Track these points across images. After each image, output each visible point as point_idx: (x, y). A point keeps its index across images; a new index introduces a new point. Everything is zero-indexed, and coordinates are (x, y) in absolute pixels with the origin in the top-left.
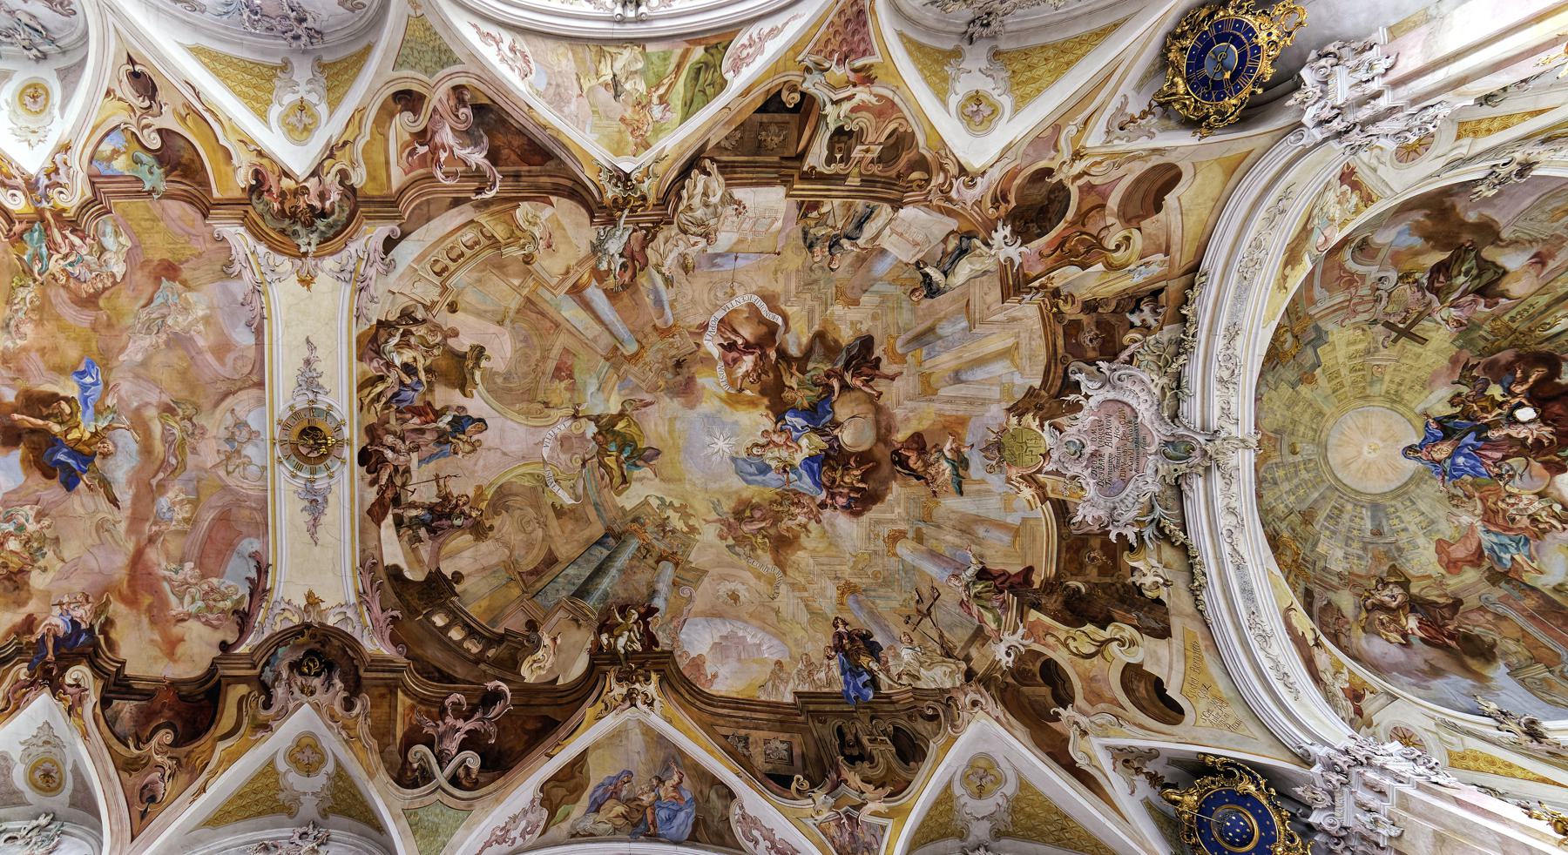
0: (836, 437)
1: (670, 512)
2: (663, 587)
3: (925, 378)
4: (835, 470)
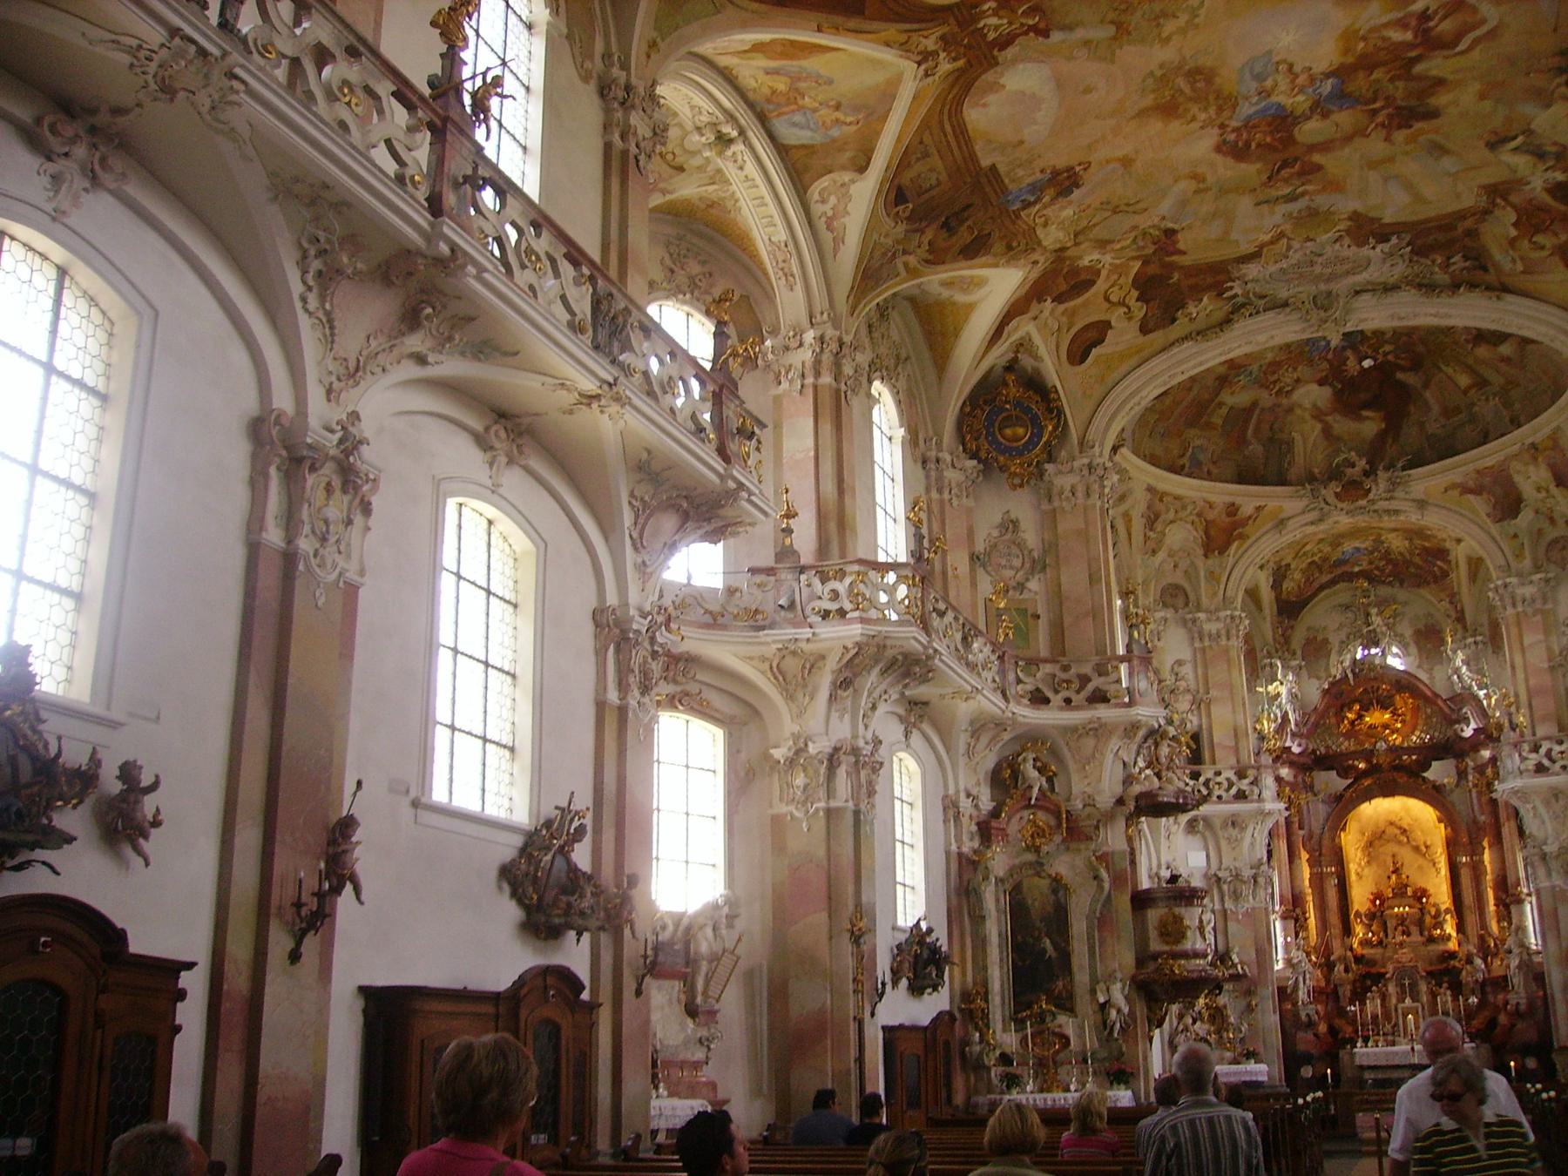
0: (1309, 118)
1: (1183, 18)
2: (1080, 34)
3: (1391, 159)
4: (1270, 124)
